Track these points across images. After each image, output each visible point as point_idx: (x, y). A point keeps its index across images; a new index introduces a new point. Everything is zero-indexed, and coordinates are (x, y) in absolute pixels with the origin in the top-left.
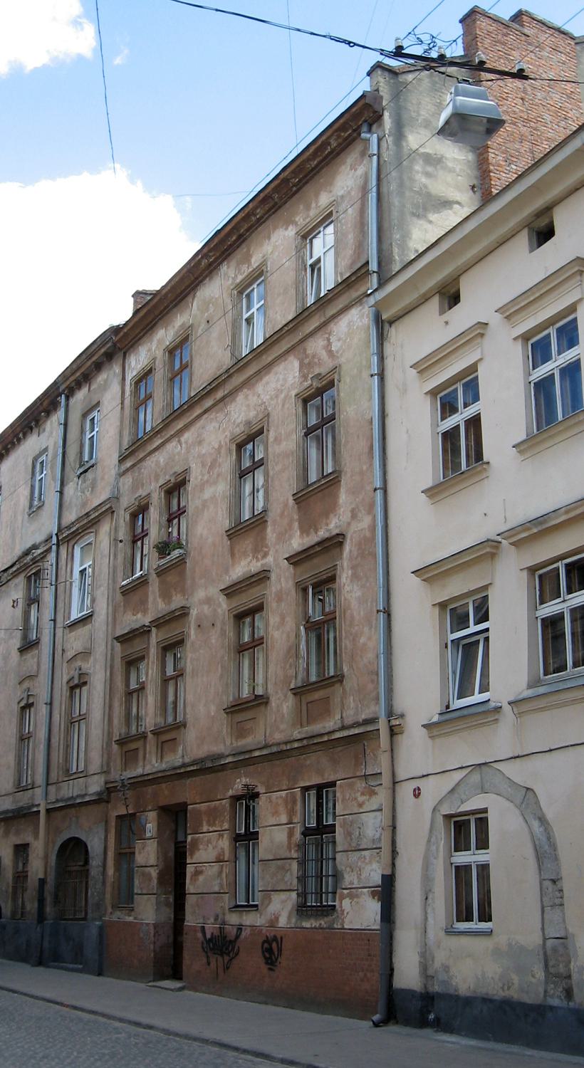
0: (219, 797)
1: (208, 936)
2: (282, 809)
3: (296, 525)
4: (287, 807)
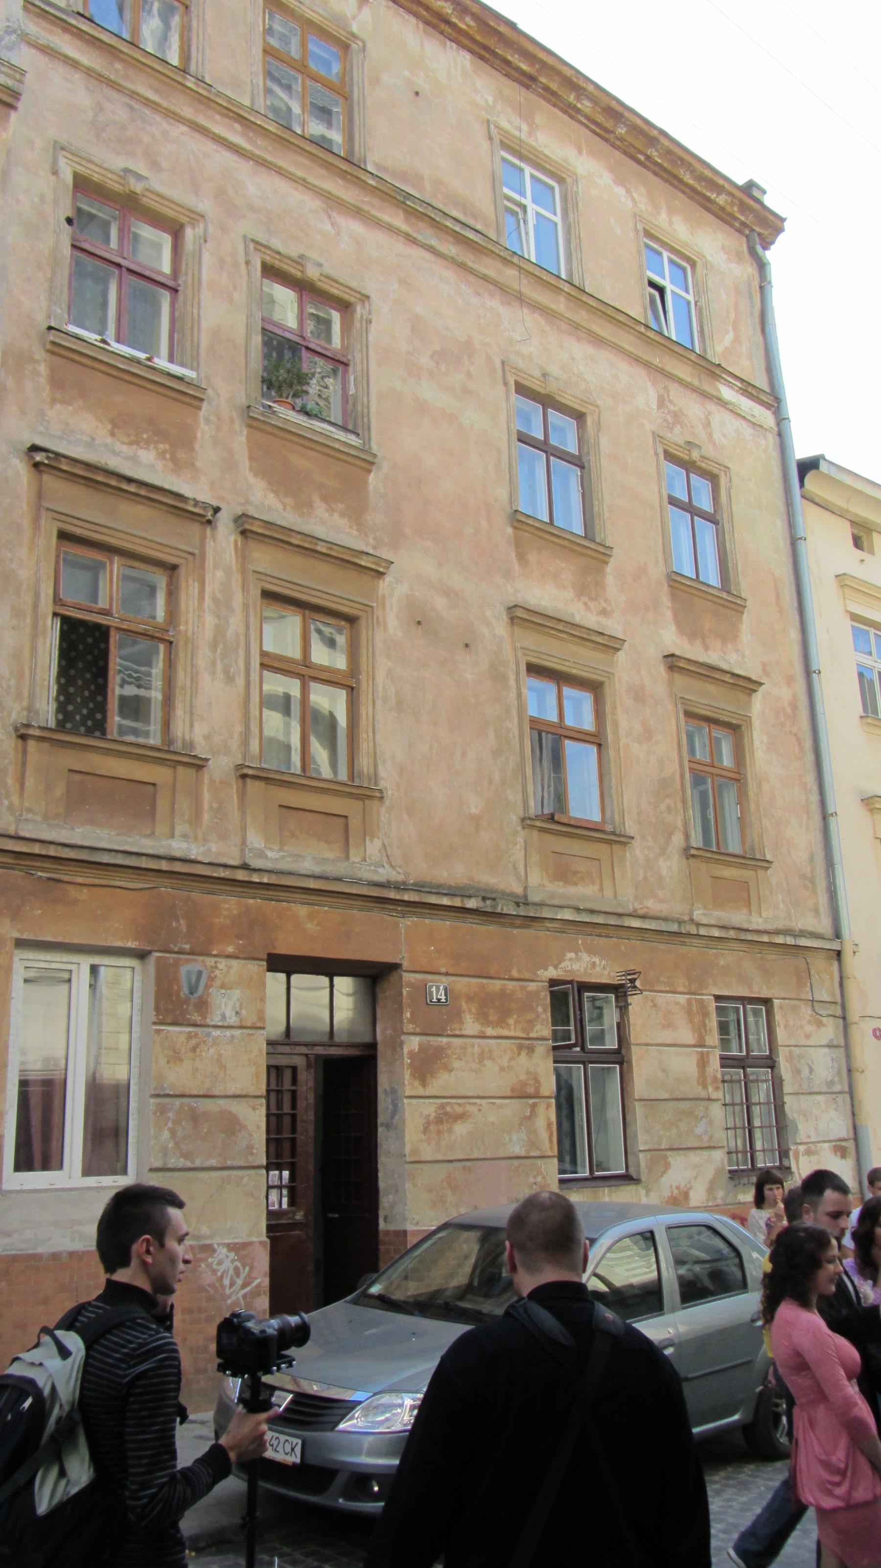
0: (515, 974)
2: (680, 1019)
3: (669, 614)
4: (691, 1021)
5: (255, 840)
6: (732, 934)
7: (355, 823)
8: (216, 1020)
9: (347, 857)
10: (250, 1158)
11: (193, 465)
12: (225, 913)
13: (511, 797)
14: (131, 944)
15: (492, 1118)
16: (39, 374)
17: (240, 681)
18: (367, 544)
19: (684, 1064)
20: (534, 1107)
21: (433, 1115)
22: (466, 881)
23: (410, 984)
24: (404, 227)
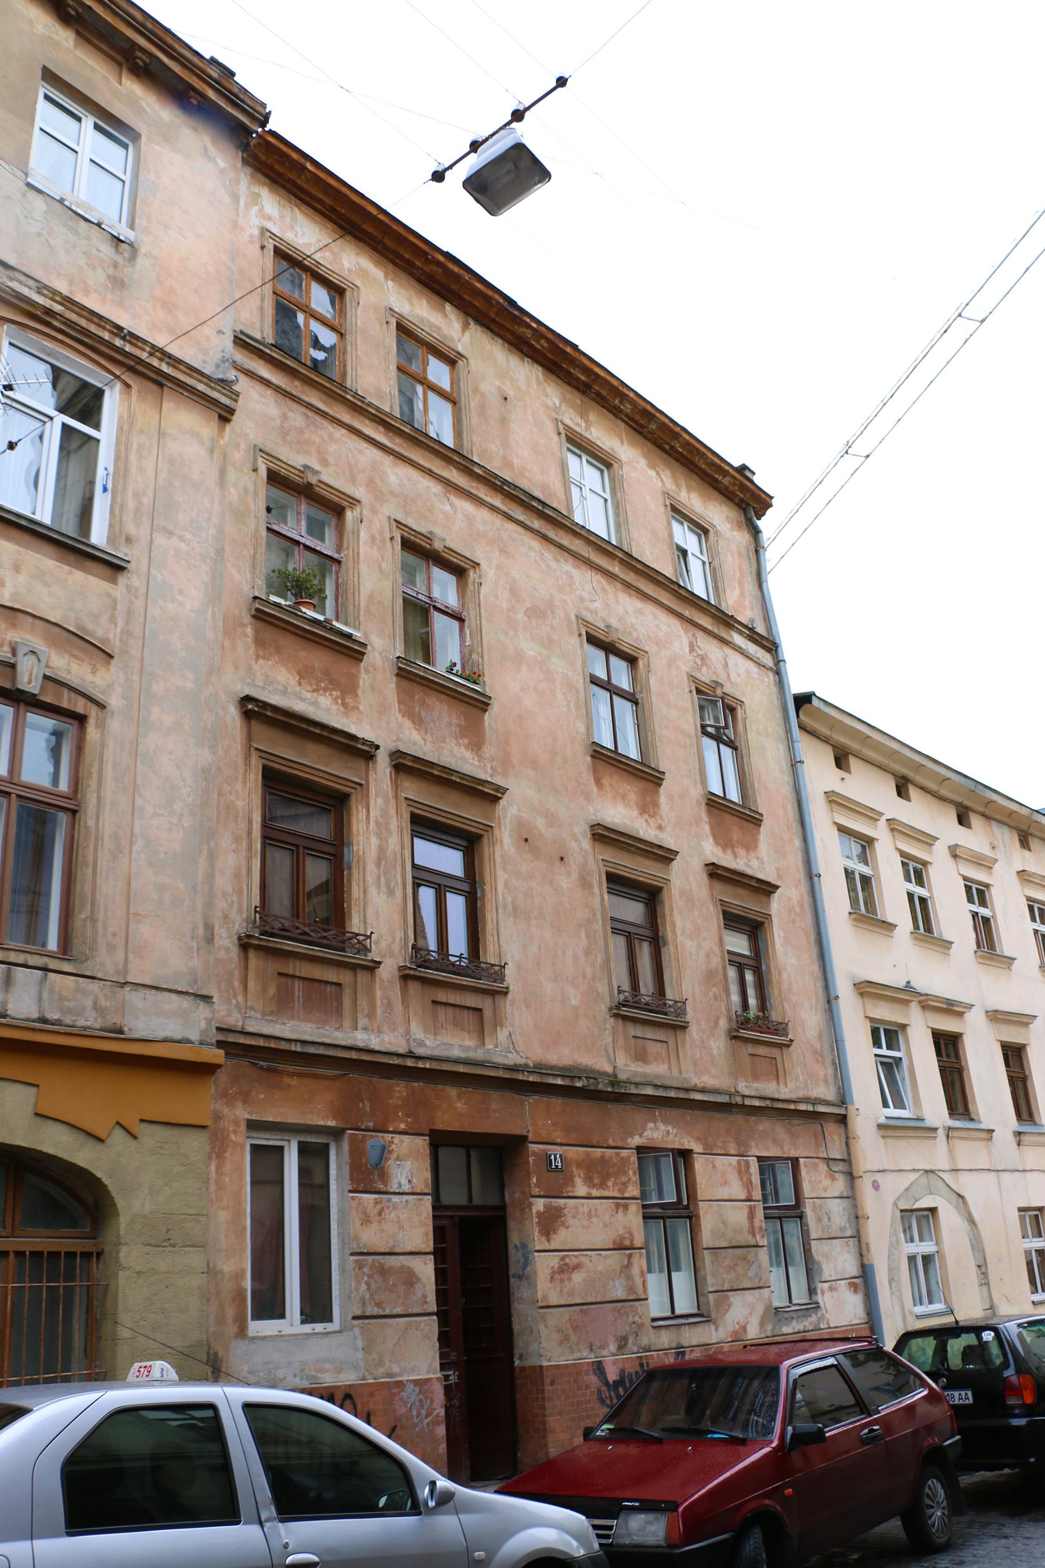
0: (612, 1143)
1: (612, 1376)
4: (741, 1179)
5: (417, 1031)
6: (768, 1103)
7: (487, 1013)
8: (394, 1188)
9: (484, 1044)
10: (425, 1306)
11: (358, 708)
12: (397, 1095)
13: (600, 990)
14: (331, 1123)
15: (600, 1268)
16: (246, 635)
17: (399, 893)
18: (486, 773)
19: (737, 1215)
20: (630, 1256)
21: (556, 1266)
22: (571, 1063)
23: (534, 1154)
24: (503, 508)
